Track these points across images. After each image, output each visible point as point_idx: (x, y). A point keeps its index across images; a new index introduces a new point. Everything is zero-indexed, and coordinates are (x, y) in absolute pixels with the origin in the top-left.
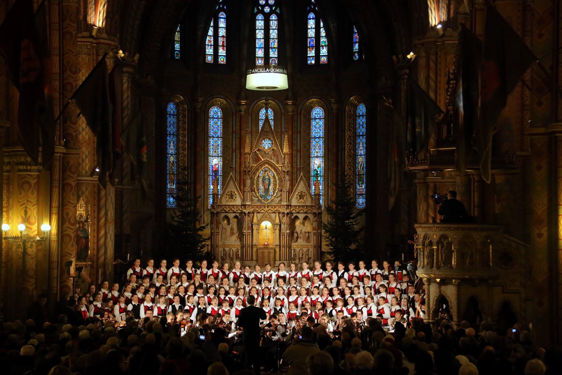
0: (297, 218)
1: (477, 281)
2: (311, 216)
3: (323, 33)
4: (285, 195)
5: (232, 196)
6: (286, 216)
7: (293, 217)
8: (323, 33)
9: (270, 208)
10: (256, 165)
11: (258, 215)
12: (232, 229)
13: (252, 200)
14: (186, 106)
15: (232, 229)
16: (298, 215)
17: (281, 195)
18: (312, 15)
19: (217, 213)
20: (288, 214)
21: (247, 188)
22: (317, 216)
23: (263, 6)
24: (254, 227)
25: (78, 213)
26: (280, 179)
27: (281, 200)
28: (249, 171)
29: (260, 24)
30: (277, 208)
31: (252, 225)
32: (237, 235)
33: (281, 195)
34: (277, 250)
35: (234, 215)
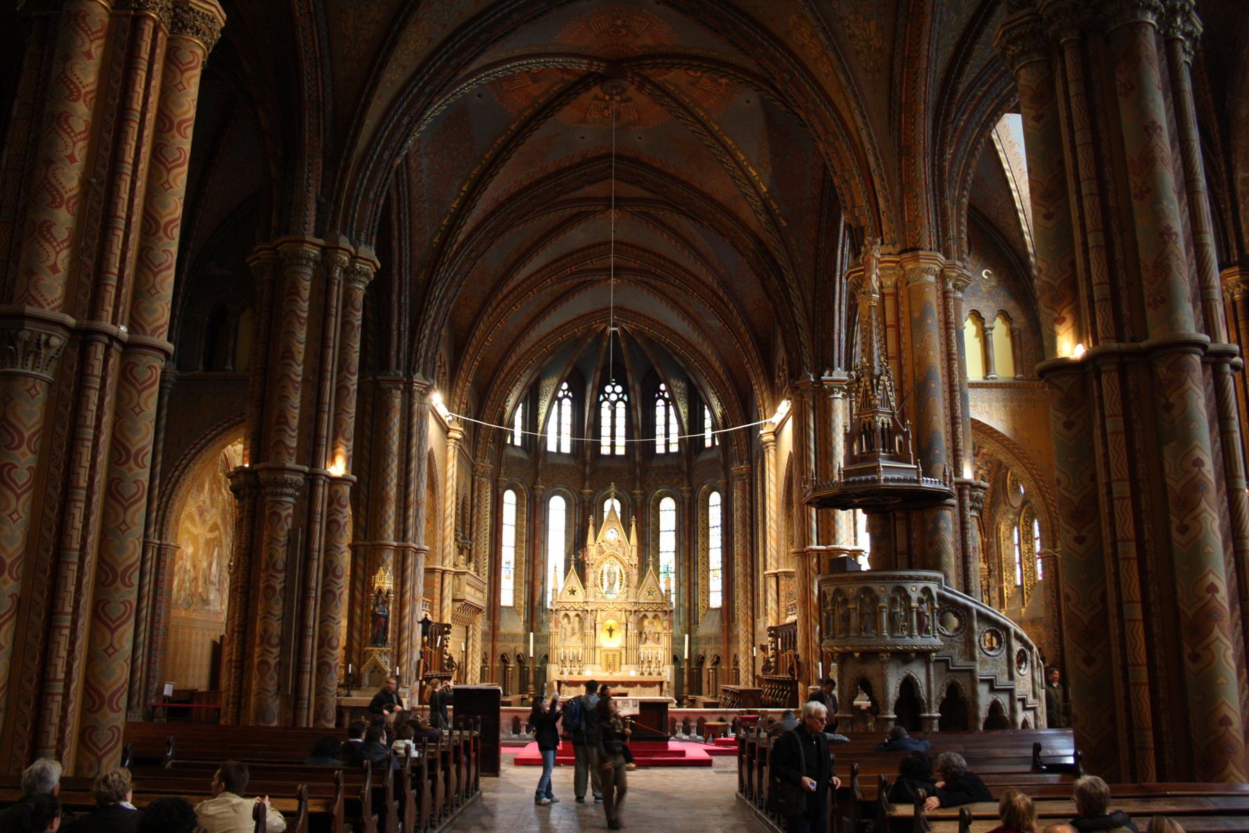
0: (645, 616)
1: (913, 655)
2: (660, 615)
3: (673, 419)
4: (632, 590)
5: (573, 592)
8: (673, 419)
12: (573, 629)
13: (595, 597)
16: (647, 614)
18: (660, 403)
21: (589, 583)
23: (609, 394)
25: (376, 585)
26: (627, 573)
34: (624, 652)
35: (575, 613)
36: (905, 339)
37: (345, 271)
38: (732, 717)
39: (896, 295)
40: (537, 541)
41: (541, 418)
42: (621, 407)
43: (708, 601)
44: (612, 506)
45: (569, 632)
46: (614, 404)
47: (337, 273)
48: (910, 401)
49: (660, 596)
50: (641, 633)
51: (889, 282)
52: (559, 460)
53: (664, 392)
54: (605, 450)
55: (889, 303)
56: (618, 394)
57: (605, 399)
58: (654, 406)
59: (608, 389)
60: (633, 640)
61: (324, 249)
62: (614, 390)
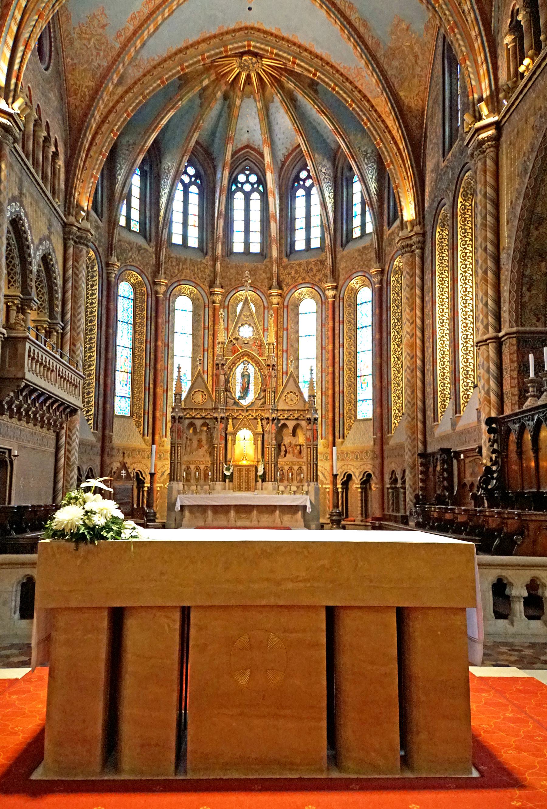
2: (303, 423)
6: (271, 422)
7: (280, 425)
9: (250, 412)
10: (231, 358)
11: (235, 421)
12: (200, 441)
13: (226, 402)
14: (145, 289)
15: (200, 441)
16: (287, 422)
17: (265, 397)
18: (301, 192)
19: (180, 418)
20: (274, 419)
22: (312, 423)
23: (242, 184)
24: (230, 438)
27: (264, 403)
28: (223, 365)
30: (260, 412)
31: (226, 434)
32: (206, 447)
33: (265, 397)
35: (202, 421)
38: (527, 576)
40: (159, 343)
41: (163, 200)
43: (356, 411)
45: (195, 443)
46: (247, 196)
49: (301, 402)
50: (279, 446)
52: (183, 255)
53: (304, 181)
54: (238, 247)
56: (252, 184)
57: (238, 190)
58: (293, 198)
59: (242, 178)
60: (270, 452)
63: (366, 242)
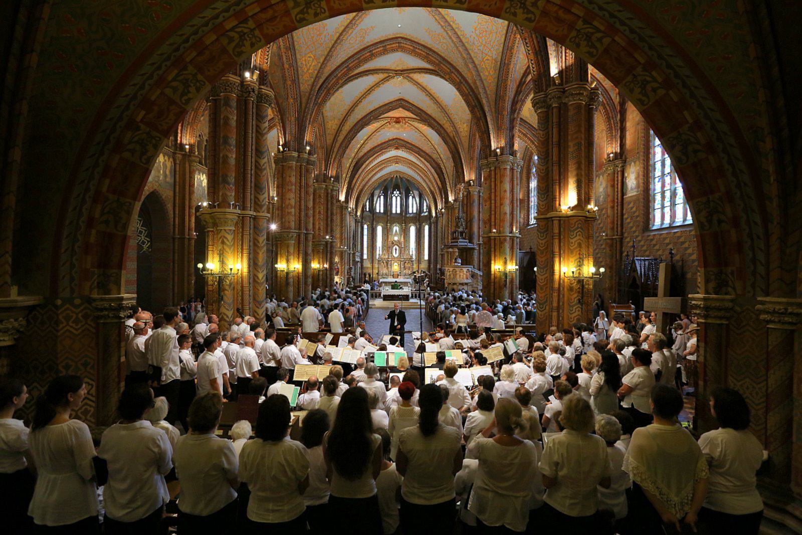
18: (411, 197)
29: (394, 198)
36: (469, 208)
37: (332, 190)
39: (467, 196)
41: (375, 202)
42: (399, 198)
44: (396, 228)
46: (396, 197)
47: (330, 191)
48: (469, 224)
51: (465, 193)
54: (394, 212)
55: (465, 198)
59: (395, 192)
61: (326, 185)
62: (396, 193)
63: (426, 214)
